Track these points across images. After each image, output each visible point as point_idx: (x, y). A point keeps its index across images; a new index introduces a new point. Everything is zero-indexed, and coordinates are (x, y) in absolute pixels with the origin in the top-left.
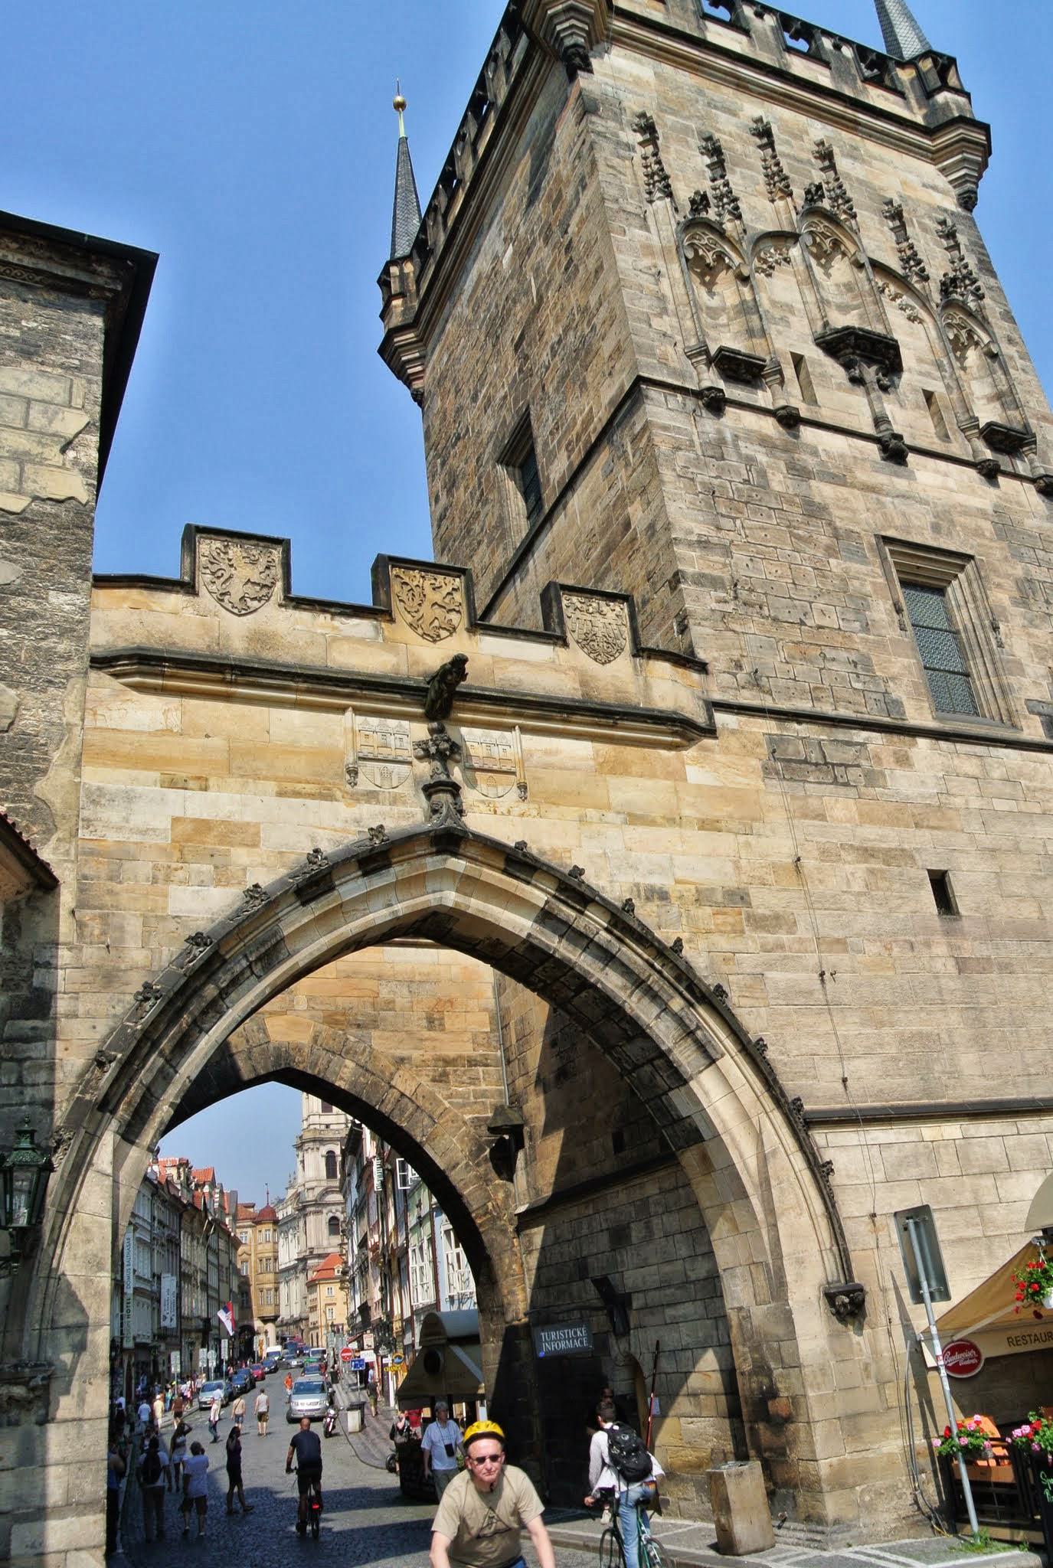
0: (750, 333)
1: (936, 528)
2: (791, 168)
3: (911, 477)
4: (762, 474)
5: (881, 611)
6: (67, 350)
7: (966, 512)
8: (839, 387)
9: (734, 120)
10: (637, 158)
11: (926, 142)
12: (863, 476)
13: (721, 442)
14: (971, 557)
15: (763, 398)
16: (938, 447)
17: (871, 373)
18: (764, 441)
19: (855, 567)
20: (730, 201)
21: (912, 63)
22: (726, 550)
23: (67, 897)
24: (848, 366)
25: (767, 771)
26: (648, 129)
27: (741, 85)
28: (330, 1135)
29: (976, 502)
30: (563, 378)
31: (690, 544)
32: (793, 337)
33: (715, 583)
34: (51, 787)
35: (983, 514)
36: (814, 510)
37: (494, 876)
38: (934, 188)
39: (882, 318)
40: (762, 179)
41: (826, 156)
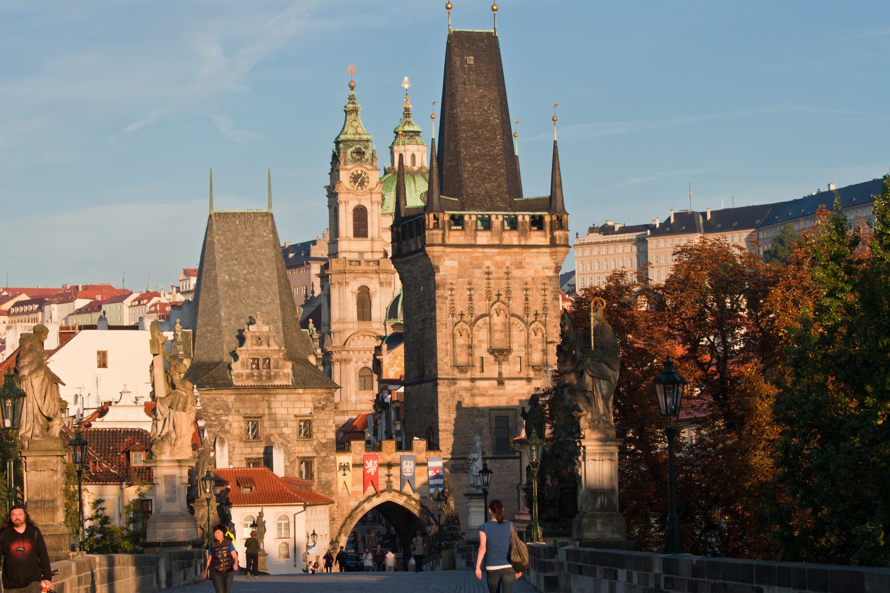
3: (505, 389)
5: (486, 430)
6: (329, 406)
7: (518, 395)
9: (480, 271)
10: (448, 302)
12: (490, 392)
15: (468, 375)
17: (501, 358)
18: (467, 389)
20: (471, 309)
28: (363, 267)
29: (523, 391)
32: (482, 351)
33: (446, 430)
34: (333, 488)
35: (523, 394)
38: (547, 268)
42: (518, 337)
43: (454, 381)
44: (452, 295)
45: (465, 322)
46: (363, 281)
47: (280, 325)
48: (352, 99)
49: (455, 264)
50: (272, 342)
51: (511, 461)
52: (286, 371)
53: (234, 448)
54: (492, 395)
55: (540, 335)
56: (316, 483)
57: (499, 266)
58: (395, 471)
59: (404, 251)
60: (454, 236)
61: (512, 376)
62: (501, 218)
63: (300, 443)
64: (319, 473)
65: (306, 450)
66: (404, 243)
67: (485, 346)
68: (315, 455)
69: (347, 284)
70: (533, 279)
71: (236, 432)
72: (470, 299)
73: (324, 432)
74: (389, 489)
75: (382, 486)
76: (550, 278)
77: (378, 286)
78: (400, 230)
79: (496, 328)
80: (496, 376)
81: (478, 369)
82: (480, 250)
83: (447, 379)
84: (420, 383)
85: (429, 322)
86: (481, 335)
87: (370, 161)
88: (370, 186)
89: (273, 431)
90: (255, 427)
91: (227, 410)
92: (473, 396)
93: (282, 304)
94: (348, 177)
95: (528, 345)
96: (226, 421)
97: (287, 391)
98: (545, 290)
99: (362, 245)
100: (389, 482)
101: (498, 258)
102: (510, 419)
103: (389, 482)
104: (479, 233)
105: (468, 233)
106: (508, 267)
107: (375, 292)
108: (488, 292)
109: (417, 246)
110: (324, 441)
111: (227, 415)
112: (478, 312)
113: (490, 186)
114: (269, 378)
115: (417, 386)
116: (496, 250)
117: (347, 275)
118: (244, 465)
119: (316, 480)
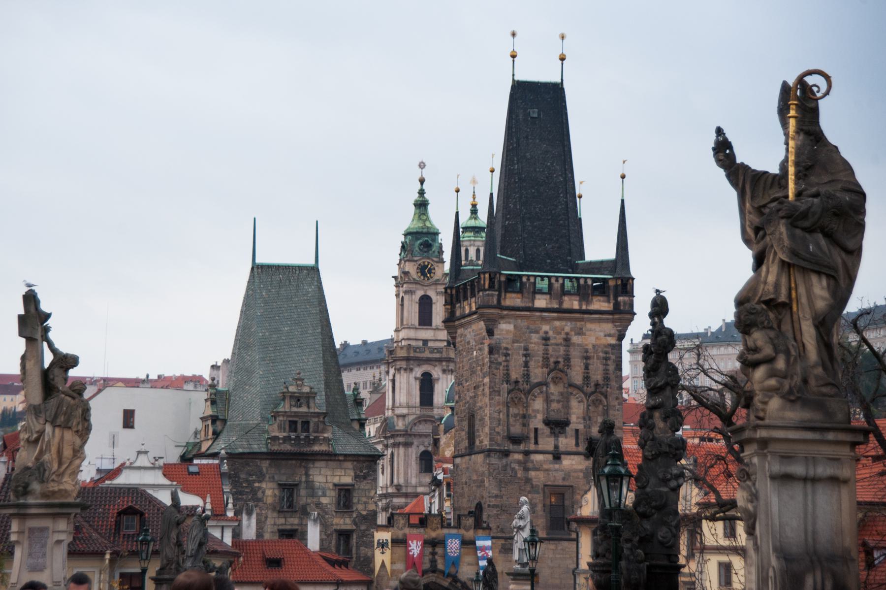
0: (524, 425)
1: (564, 479)
2: (554, 350)
3: (561, 463)
4: (516, 473)
7: (576, 471)
8: (547, 436)
9: (537, 336)
10: (501, 368)
11: (611, 317)
12: (545, 467)
13: (507, 465)
14: (572, 486)
15: (522, 447)
16: (574, 449)
17: (557, 430)
18: (519, 462)
19: (536, 496)
20: (527, 376)
21: (616, 279)
22: (502, 497)
23: (375, 583)
24: (551, 429)
25: (500, 552)
26: (507, 355)
27: (543, 319)
28: (427, 354)
29: (581, 467)
30: (480, 420)
31: (493, 497)
32: (537, 422)
34: (371, 565)
35: (581, 471)
36: (528, 480)
37: (441, 576)
39: (567, 407)
40: (541, 359)
41: (567, 340)
42: (577, 410)
43: (506, 454)
44: (506, 361)
45: (519, 389)
46: (426, 368)
47: (323, 386)
48: (422, 192)
49: (511, 327)
50: (312, 404)
51: (565, 544)
52: (326, 435)
53: (266, 518)
54: (547, 470)
55: (601, 407)
56: (354, 559)
57: (557, 331)
58: (439, 550)
59: (458, 313)
60: (511, 298)
61: (569, 449)
62: (561, 281)
63: (339, 515)
64: (358, 547)
65: (344, 523)
66: (458, 305)
67: (540, 417)
68: (354, 527)
69: (411, 370)
70: (594, 346)
71: (270, 500)
72: (526, 364)
73: (365, 503)
74: (434, 569)
75: (427, 566)
76: (612, 346)
77: (440, 373)
78: (454, 292)
79: (553, 397)
80: (551, 448)
81: (533, 441)
82: (538, 314)
83: (500, 451)
84: (470, 455)
85: (481, 389)
86: (538, 404)
87: (436, 253)
88: (436, 278)
89: (309, 501)
90: (291, 495)
91: (261, 477)
92: (526, 470)
93: (325, 363)
94: (416, 267)
95: (587, 418)
96: (259, 488)
97: (327, 458)
98: (606, 359)
99: (426, 334)
100: (433, 562)
101: (557, 323)
102: (566, 496)
103: (433, 562)
104: (537, 296)
105: (526, 295)
106: (567, 334)
107: (438, 379)
108: (546, 359)
109: (471, 308)
110: (364, 513)
111: (260, 482)
112: (534, 380)
113: (550, 246)
114: (309, 442)
115: (467, 458)
116: (555, 315)
117: (412, 362)
118: (276, 537)
119: (354, 556)
